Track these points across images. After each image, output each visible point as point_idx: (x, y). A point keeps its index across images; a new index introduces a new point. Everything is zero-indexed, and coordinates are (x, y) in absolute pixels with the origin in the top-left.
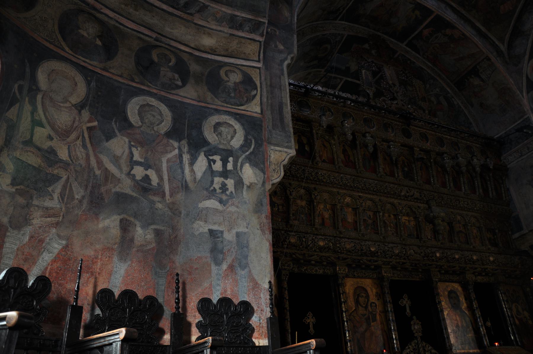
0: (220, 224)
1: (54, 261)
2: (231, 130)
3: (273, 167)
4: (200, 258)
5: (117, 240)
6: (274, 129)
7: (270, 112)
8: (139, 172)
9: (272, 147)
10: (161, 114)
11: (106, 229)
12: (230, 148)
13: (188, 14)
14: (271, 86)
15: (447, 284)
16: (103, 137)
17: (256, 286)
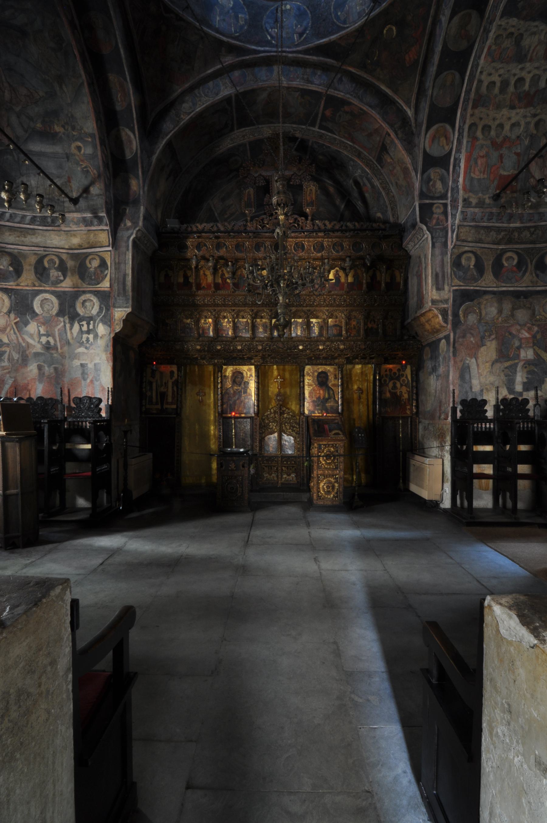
0: (86, 360)
1: (11, 387)
2: (92, 303)
3: (116, 322)
4: (76, 378)
5: (37, 375)
6: (118, 296)
7: (116, 284)
8: (44, 340)
9: (116, 309)
10: (52, 303)
11: (31, 371)
12: (91, 315)
13: (56, 226)
14: (119, 263)
15: (320, 366)
16: (23, 326)
17: (103, 389)
